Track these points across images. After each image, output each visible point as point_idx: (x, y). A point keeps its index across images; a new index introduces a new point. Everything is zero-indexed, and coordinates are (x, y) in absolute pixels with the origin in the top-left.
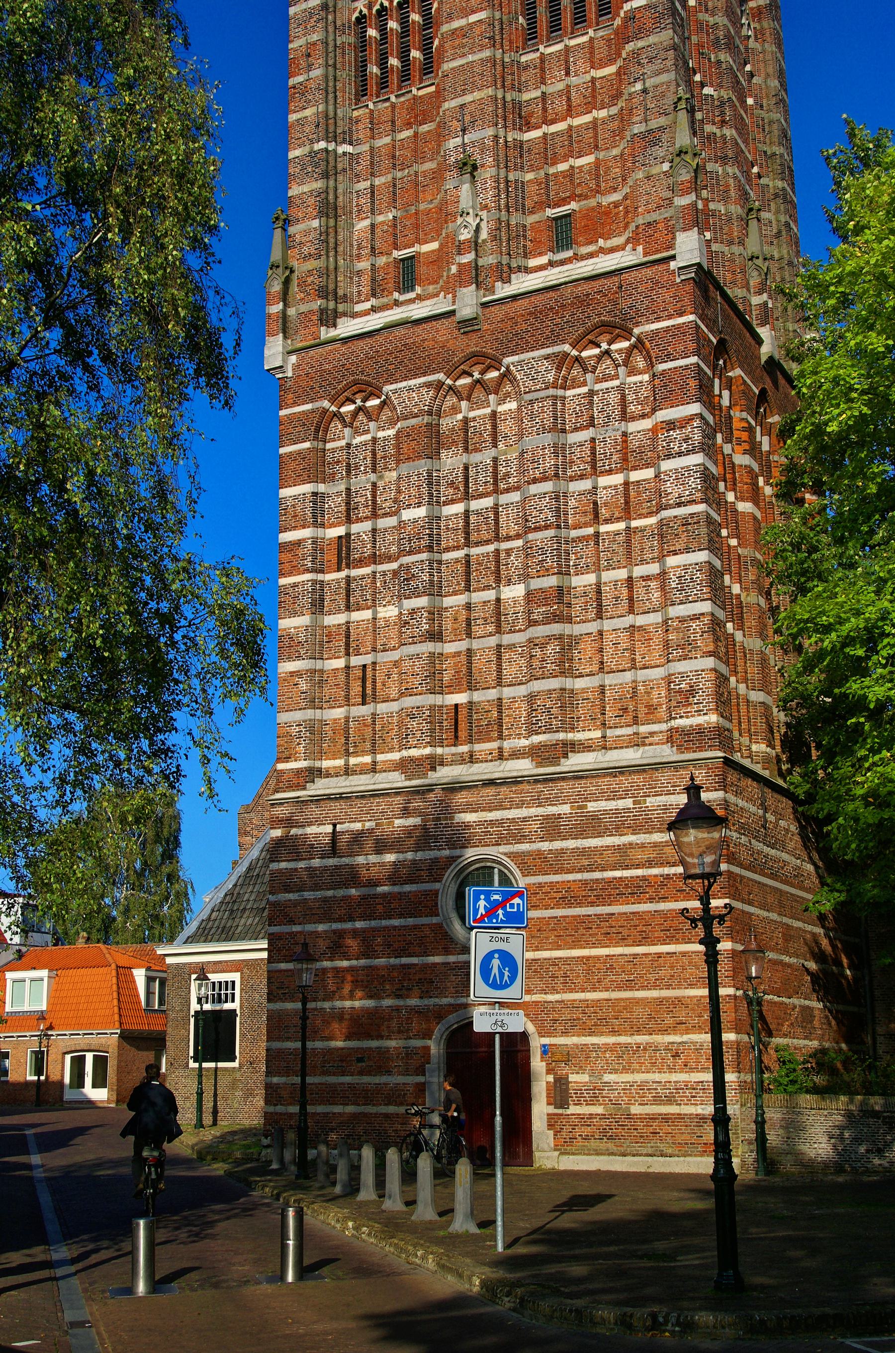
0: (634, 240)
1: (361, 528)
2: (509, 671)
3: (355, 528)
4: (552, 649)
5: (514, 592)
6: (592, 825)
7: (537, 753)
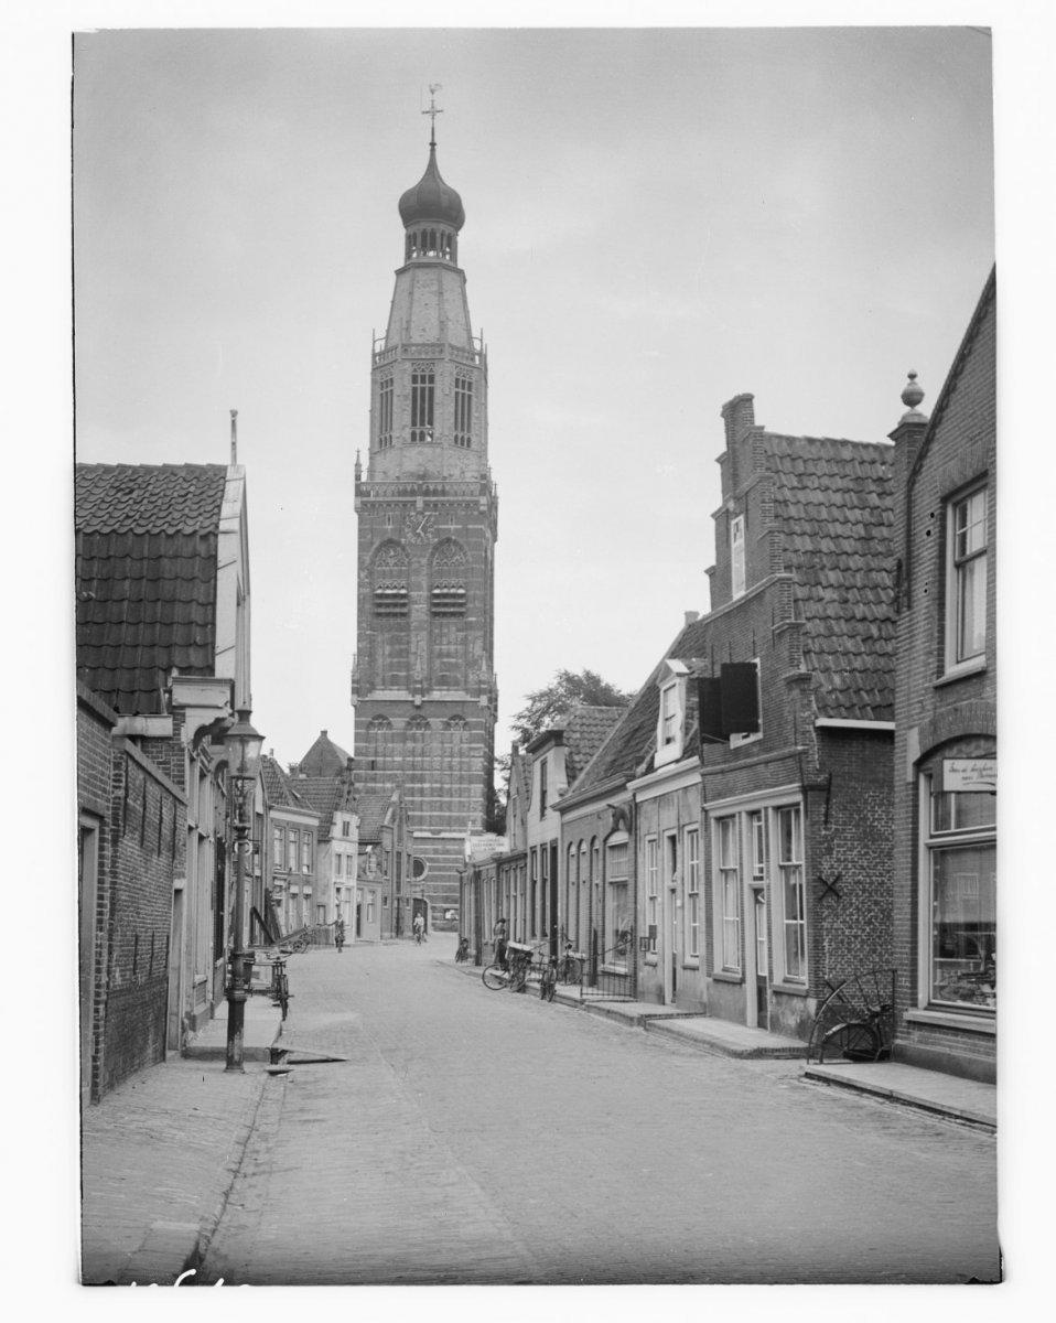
0: (467, 691)
1: (380, 759)
2: (424, 808)
3: (378, 759)
4: (438, 804)
5: (426, 785)
6: (447, 852)
7: (433, 832)
